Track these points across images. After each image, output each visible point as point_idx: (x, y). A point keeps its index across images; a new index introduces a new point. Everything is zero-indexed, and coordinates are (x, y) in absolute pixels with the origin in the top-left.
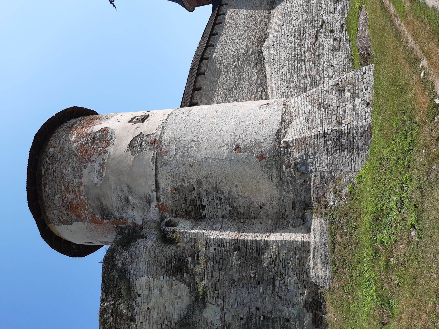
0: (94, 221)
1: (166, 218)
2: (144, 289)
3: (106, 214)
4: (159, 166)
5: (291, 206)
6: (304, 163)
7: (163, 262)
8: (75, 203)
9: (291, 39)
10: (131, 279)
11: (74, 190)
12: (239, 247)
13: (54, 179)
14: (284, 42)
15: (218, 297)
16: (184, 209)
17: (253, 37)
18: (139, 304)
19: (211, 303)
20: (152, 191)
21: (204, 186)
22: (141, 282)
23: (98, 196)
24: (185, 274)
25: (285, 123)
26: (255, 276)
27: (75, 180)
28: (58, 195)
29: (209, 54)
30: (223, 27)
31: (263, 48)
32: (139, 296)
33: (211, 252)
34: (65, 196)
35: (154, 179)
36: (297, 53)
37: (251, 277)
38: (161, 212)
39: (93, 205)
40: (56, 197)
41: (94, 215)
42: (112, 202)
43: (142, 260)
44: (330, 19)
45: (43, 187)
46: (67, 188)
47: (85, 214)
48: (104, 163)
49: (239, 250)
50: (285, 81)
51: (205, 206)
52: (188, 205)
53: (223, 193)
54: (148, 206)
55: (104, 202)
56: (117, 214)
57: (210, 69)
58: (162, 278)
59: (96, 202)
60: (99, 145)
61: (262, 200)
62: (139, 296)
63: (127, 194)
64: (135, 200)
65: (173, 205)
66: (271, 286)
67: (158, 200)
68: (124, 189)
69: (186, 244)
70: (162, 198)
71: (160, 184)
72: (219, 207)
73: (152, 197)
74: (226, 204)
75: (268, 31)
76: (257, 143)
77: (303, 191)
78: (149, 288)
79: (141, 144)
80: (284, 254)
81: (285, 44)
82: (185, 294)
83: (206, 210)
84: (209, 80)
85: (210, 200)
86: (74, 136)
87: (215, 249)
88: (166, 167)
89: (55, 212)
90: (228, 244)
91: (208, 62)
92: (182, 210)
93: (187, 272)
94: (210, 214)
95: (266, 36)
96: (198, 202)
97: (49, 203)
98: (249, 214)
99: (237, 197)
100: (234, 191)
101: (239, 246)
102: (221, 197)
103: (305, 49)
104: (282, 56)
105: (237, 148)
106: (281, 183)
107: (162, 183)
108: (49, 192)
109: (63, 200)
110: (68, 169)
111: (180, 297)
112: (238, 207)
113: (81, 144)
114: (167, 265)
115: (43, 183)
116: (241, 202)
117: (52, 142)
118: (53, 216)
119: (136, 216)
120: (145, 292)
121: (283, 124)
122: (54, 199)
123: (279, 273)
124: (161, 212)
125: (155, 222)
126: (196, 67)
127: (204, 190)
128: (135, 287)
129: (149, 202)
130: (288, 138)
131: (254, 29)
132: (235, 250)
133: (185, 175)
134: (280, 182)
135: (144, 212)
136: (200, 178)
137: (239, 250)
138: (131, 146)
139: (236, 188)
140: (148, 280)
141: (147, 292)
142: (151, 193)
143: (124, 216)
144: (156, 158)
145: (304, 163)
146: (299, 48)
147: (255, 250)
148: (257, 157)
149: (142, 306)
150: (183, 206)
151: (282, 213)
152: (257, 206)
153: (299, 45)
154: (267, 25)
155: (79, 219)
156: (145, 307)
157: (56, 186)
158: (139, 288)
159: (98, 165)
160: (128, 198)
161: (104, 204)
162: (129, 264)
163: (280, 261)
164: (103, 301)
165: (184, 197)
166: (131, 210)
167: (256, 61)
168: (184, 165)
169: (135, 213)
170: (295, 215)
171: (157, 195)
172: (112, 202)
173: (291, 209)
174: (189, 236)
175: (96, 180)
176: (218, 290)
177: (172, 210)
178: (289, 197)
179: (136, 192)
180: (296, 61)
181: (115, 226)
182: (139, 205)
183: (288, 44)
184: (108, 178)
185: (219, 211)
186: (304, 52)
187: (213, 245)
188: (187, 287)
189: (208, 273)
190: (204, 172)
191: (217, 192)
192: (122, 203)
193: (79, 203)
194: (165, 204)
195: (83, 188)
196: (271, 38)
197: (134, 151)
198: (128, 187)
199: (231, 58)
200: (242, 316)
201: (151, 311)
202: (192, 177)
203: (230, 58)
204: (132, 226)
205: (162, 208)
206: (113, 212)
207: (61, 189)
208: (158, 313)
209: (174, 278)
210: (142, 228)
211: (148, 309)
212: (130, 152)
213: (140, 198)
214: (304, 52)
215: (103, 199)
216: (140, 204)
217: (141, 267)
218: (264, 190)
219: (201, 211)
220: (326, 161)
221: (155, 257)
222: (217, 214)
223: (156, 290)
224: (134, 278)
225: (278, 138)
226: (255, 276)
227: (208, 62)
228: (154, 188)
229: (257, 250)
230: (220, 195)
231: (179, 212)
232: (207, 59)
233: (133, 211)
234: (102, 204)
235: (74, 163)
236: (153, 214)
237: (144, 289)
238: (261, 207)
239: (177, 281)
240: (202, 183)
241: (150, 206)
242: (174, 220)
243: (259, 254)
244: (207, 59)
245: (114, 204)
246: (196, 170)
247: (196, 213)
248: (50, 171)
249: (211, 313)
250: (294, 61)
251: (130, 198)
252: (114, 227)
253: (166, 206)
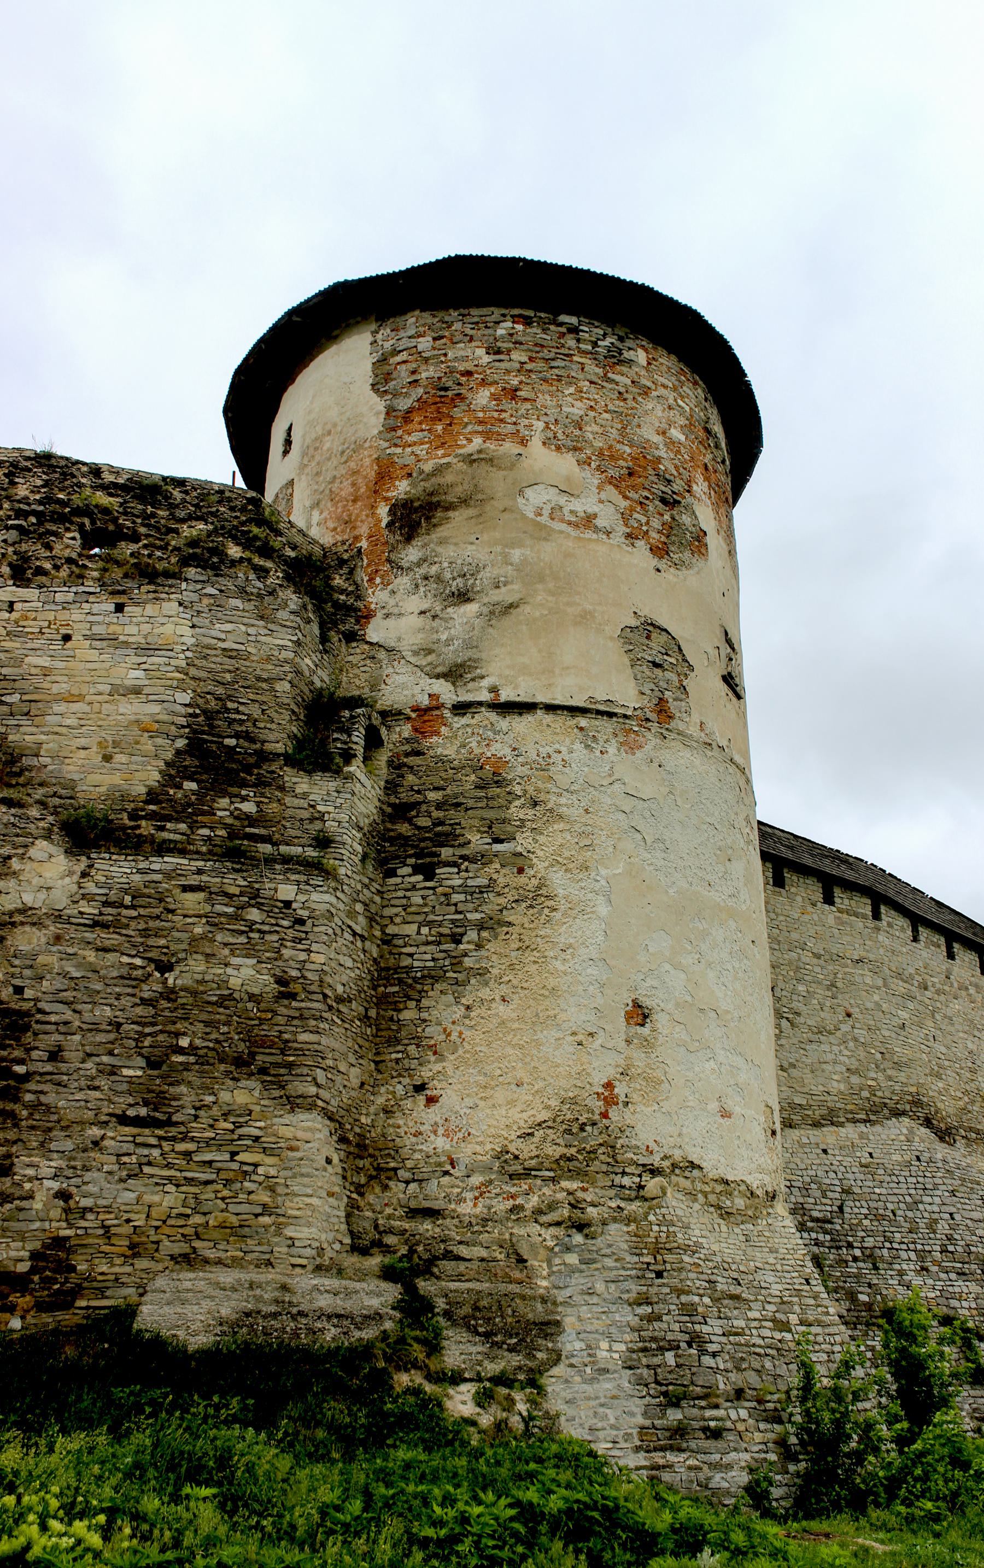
0: (385, 472)
1: (389, 728)
2: (146, 628)
3: (413, 518)
4: (583, 722)
5: (426, 1204)
7: (241, 708)
8: (457, 412)
9: (943, 1227)
10: (184, 585)
11: (504, 415)
12: (293, 996)
13: (545, 353)
14: (928, 1199)
15: (106, 904)
16: (419, 798)
17: (940, 1085)
18: (85, 605)
19: (84, 875)
20: (494, 690)
21: (504, 877)
22: (169, 621)
23: (480, 496)
24: (193, 786)
26: (181, 1051)
27: (540, 425)
28: (486, 359)
29: (890, 925)
31: (906, 1120)
32: (119, 608)
33: (276, 890)
34: (484, 383)
35: (540, 699)
36: (896, 1246)
37: (178, 1035)
38: (414, 715)
39: (449, 478)
40: (481, 352)
41: (410, 475)
42: (456, 544)
43: (252, 631)
45: (516, 312)
46: (513, 393)
47: (415, 444)
48: (597, 530)
49: (283, 995)
50: (801, 1200)
51: (427, 879)
52: (436, 814)
53: (479, 946)
54: (440, 670)
55: (458, 516)
56: (411, 554)
57: (842, 923)
58: (186, 698)
59: (459, 490)
60: (656, 523)
61: (450, 1098)
62: (119, 608)
63: (486, 600)
64: (461, 624)
65: (441, 760)
66: (143, 1111)
67: (461, 708)
68: (503, 589)
69: (305, 796)
70: (464, 720)
71: (517, 718)
72: (425, 930)
73: (471, 685)
74: (436, 956)
75: (960, 1143)
77: (484, 1253)
78: (147, 649)
79: (656, 665)
80: (261, 1170)
81: (921, 1202)
82: (117, 779)
83: (414, 879)
84: (806, 918)
85: (456, 898)
86: (682, 438)
87: (288, 904)
88: (578, 746)
89: (425, 344)
90: (303, 956)
91: (864, 917)
92: (419, 792)
93: (200, 795)
94: (400, 894)
95: (945, 1135)
96: (446, 853)
97: (457, 326)
98: (394, 1041)
99: (464, 1001)
100: (485, 993)
102: (465, 939)
103: (910, 1276)
104: (884, 1191)
106: (514, 1169)
108: (500, 332)
109: (469, 373)
110: (578, 404)
111: (107, 758)
112: (425, 1002)
113: (659, 460)
114: (231, 722)
115: (530, 313)
116: (441, 1009)
117: (666, 361)
118: (412, 332)
120: (133, 629)
121: (719, 1188)
122: (467, 344)
123: (191, 1146)
124: (414, 715)
125: (374, 687)
126: (849, 875)
127: (495, 876)
128: (151, 596)
129: (454, 674)
130: (675, 1204)
131: (966, 1093)
132: (281, 981)
133: (551, 811)
134: (517, 1168)
135: (416, 653)
136: (540, 866)
137: (283, 995)
139: (498, 998)
140: (178, 648)
141: (131, 639)
142: (485, 683)
143: (403, 582)
144: (611, 715)
146: (913, 1255)
147: (279, 1059)
148: (609, 1085)
149: (76, 615)
150: (432, 796)
151: (395, 1170)
152: (425, 1073)
153: (922, 1255)
155: (397, 421)
156: (76, 626)
157: (519, 356)
158: (150, 609)
159: (590, 511)
160: (469, 600)
161: (451, 514)
162: (240, 582)
163: (234, 1154)
164: (96, 471)
165: (471, 803)
166: (425, 606)
167: (865, 1094)
168: (587, 811)
169: (415, 621)
170: (389, 1217)
171: (480, 704)
172: (456, 544)
173: (413, 1204)
174: (331, 809)
176: (133, 907)
177: (418, 753)
178: (460, 1200)
179: (491, 630)
180: (870, 1242)
181: (364, 544)
182: (444, 637)
183: (926, 1215)
184: (545, 539)
185: (411, 929)
186: (901, 1273)
187: (301, 898)
188: (143, 790)
189: (200, 872)
190: (559, 881)
191: (481, 926)
192: (454, 579)
193: (455, 428)
194: (443, 730)
195: (510, 447)
196: (941, 1151)
197: (635, 637)
198: (511, 606)
199: (877, 1003)
200: (28, 993)
201: (58, 645)
202: (542, 839)
203: (876, 998)
204: (360, 604)
205: (426, 716)
206: (418, 542)
207: (508, 372)
208: (46, 672)
209: (181, 743)
210: (351, 637)
211: (67, 638)
212: (633, 622)
213: (469, 645)
214: (901, 1273)
215: (471, 512)
216: (448, 642)
217: (229, 627)
219: (412, 861)
220: (604, 1345)
221: (259, 679)
222: (398, 920)
223: (139, 674)
224: (188, 596)
225: (674, 1166)
226: (181, 1051)
227: (864, 917)
228: (506, 695)
229: (277, 1065)
230: (472, 935)
231: (411, 778)
232: (876, 916)
233: (423, 613)
234: (450, 507)
235: (596, 428)
236: (404, 687)
237: (146, 628)
238: (419, 1088)
239: (169, 756)
240: (521, 871)
241: (438, 677)
242: (382, 757)
243: (263, 1071)
244: (876, 916)
245: (448, 552)
246: (567, 854)
248: (572, 343)
249: (49, 874)
250: (870, 1233)
251: (471, 608)
252: (357, 538)
253: (438, 733)
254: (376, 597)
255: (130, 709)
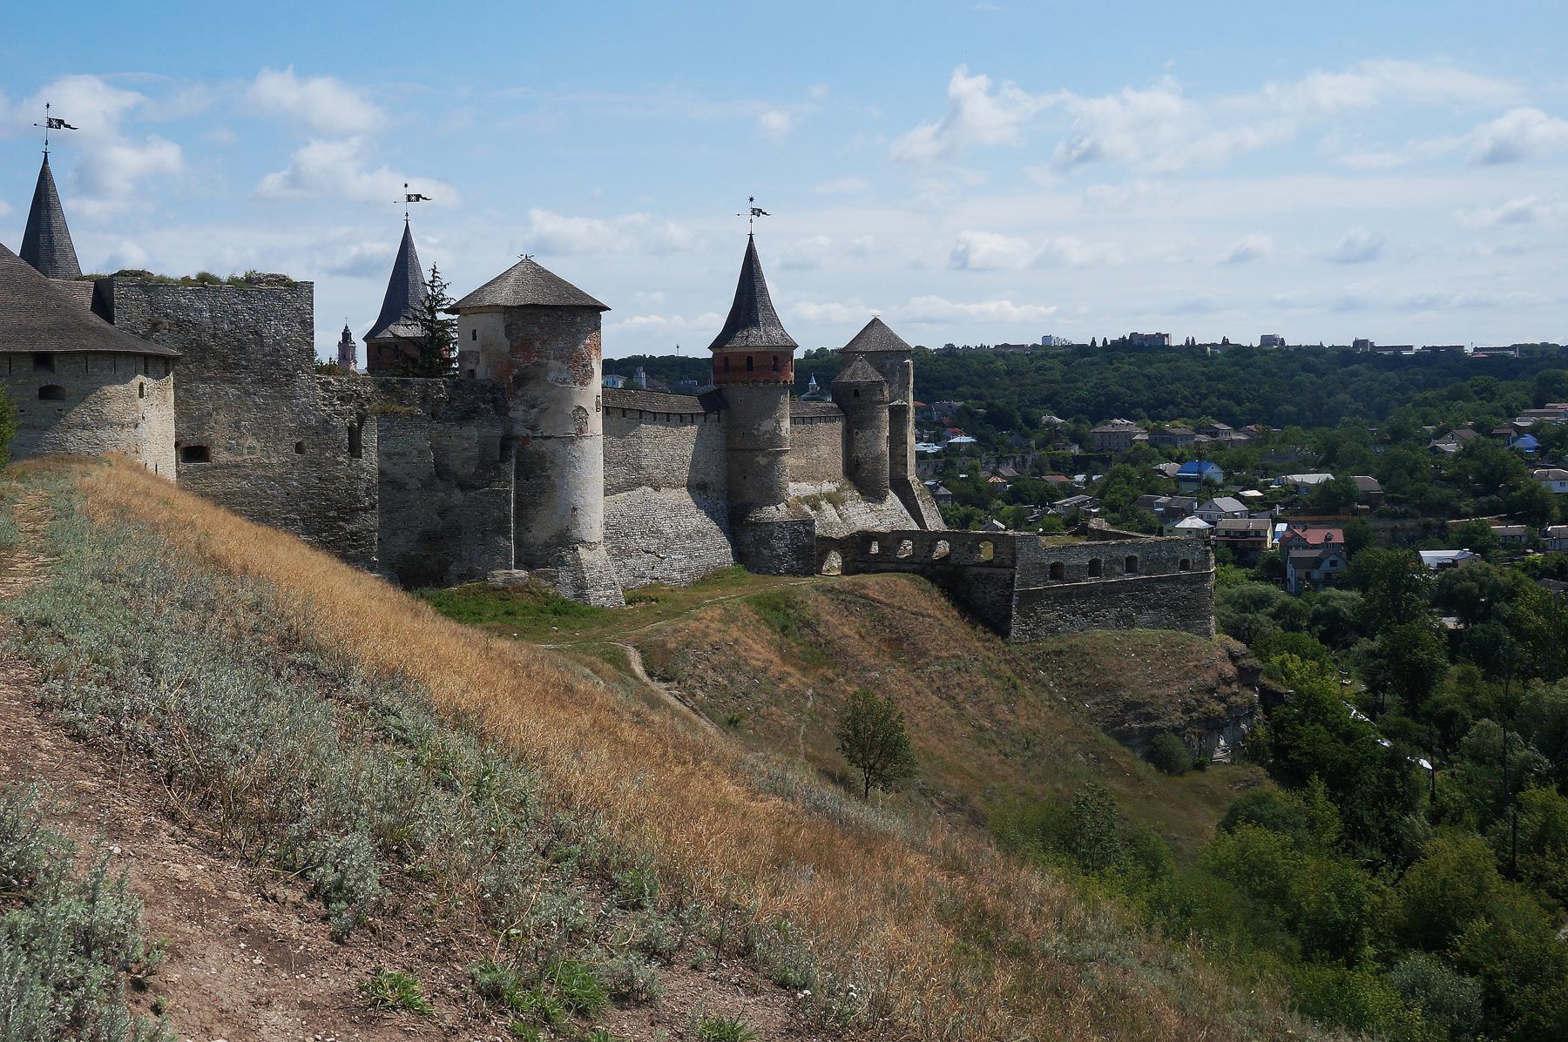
3: (520, 381)
6: (563, 564)
25: (589, 546)
30: (677, 426)
44: (665, 565)
76: (577, 526)
95: (657, 489)
101: (507, 517)
105: (575, 509)
106: (547, 545)
107: (549, 442)
119: (518, 412)
129: (533, 428)
138: (580, 408)
145: (563, 564)
154: (670, 485)
155: (513, 350)
172: (532, 391)
175: (552, 375)
196: (655, 494)
205: (526, 439)
218: (540, 533)
247: (524, 473)
254: (511, 404)
255: (466, 454)
